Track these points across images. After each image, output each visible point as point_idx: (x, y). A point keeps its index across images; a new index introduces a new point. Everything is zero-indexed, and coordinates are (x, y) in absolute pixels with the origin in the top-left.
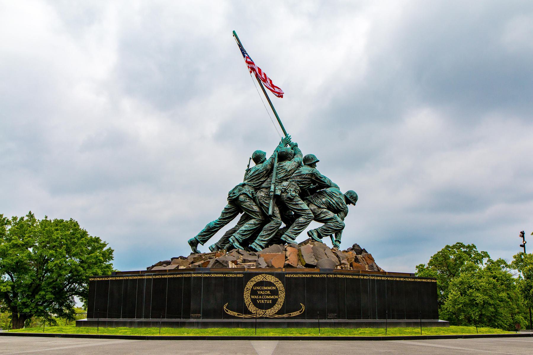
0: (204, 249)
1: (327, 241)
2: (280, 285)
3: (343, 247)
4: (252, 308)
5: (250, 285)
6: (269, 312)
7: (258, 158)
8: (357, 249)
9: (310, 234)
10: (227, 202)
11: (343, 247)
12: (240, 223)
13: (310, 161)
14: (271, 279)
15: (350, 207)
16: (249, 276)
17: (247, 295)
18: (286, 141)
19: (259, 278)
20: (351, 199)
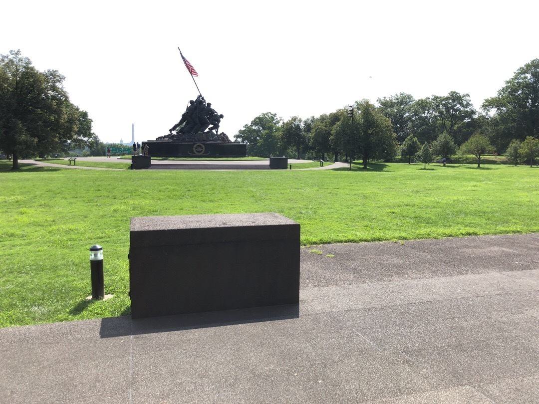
0: (174, 132)
1: (214, 131)
2: (204, 147)
3: (219, 133)
4: (196, 152)
5: (195, 146)
6: (200, 154)
7: (191, 102)
8: (223, 133)
9: (209, 129)
10: (181, 118)
11: (219, 133)
12: (186, 125)
13: (209, 104)
14: (201, 144)
15: (221, 119)
16: (195, 144)
17: (194, 149)
18: (200, 96)
19: (198, 144)
20: (222, 116)
